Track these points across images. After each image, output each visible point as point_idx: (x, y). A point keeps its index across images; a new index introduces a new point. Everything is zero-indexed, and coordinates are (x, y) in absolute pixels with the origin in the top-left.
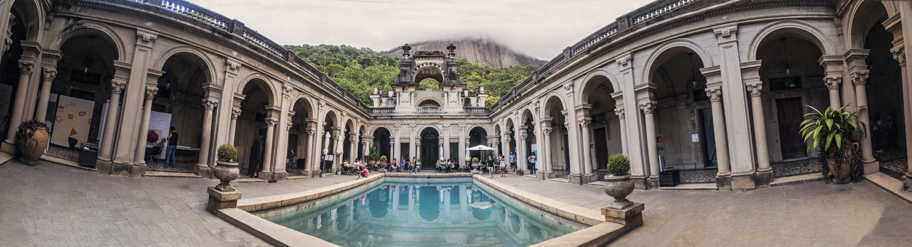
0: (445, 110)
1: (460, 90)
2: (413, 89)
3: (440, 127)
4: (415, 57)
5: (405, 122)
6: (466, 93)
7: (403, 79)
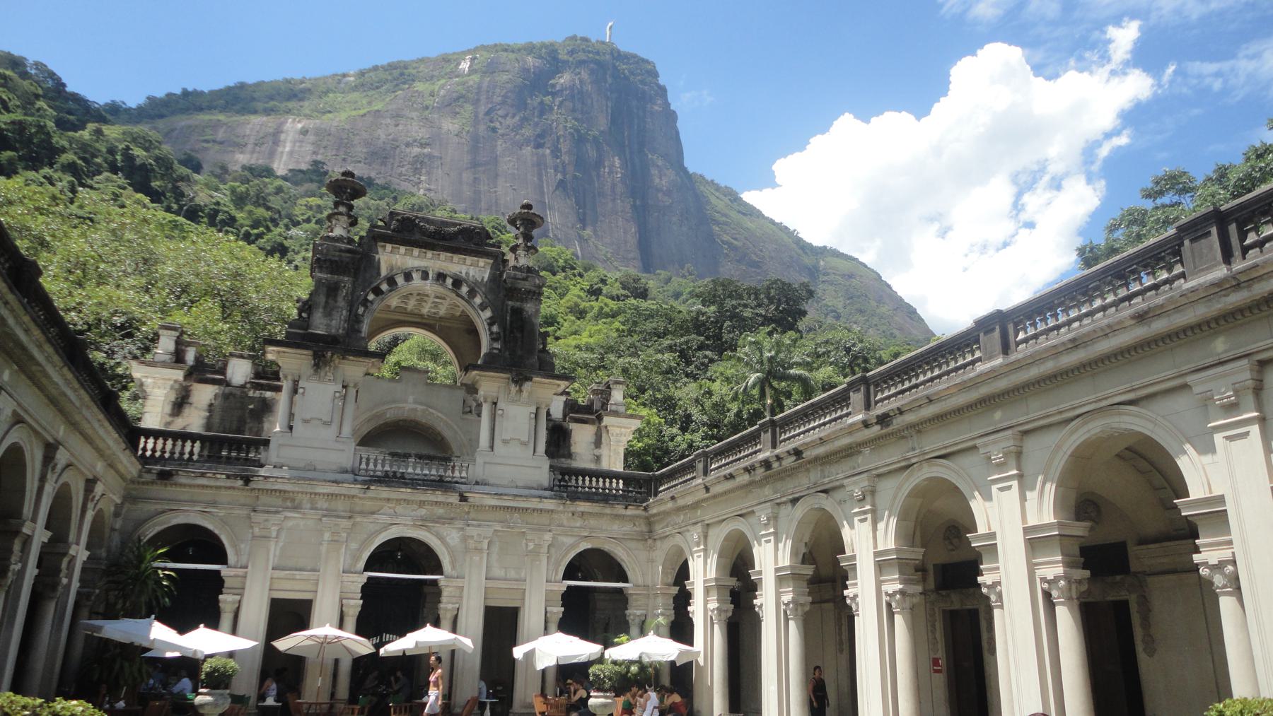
0: (478, 469)
3: (453, 535)
4: (376, 237)
7: (320, 325)
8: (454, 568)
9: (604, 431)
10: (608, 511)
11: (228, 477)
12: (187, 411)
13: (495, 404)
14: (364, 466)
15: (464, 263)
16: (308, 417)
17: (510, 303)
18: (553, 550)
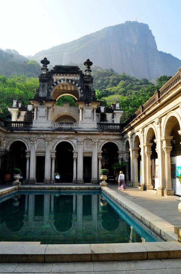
1: (95, 106)
2: (50, 105)
3: (75, 141)
5: (42, 136)
6: (102, 109)
7: (41, 94)
8: (75, 148)
9: (114, 114)
10: (111, 133)
11: (24, 130)
12: (20, 117)
13: (83, 109)
14: (53, 126)
15: (73, 76)
16: (40, 116)
17: (85, 84)
18: (99, 143)
